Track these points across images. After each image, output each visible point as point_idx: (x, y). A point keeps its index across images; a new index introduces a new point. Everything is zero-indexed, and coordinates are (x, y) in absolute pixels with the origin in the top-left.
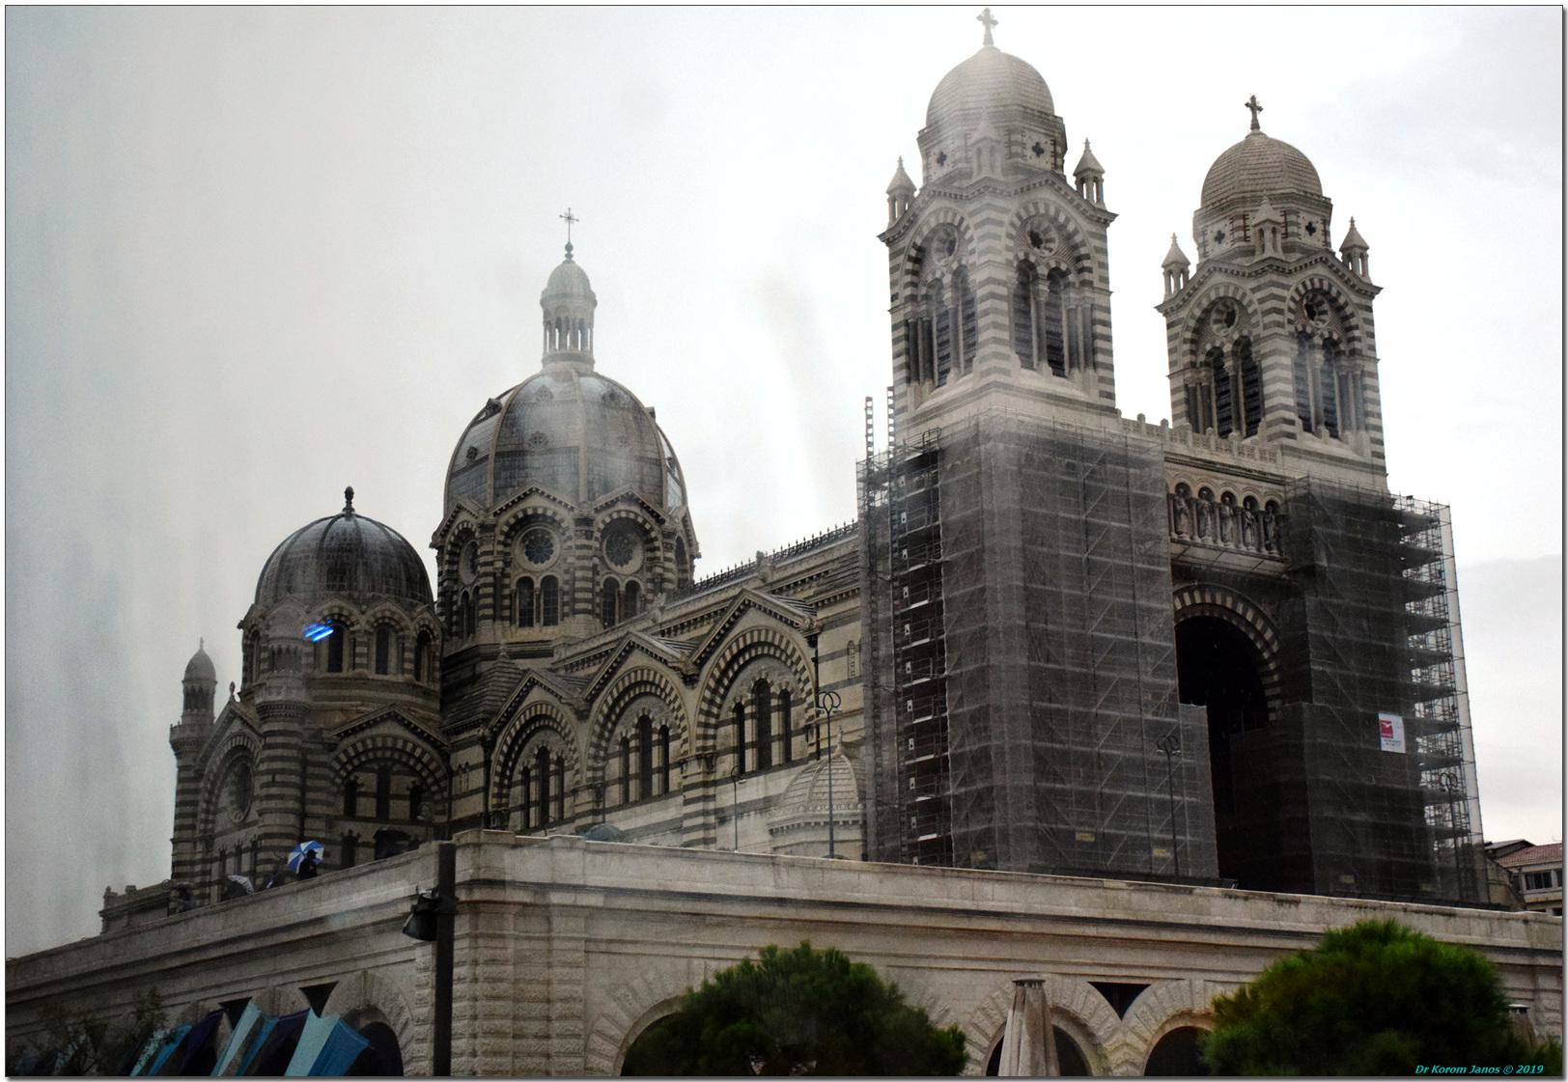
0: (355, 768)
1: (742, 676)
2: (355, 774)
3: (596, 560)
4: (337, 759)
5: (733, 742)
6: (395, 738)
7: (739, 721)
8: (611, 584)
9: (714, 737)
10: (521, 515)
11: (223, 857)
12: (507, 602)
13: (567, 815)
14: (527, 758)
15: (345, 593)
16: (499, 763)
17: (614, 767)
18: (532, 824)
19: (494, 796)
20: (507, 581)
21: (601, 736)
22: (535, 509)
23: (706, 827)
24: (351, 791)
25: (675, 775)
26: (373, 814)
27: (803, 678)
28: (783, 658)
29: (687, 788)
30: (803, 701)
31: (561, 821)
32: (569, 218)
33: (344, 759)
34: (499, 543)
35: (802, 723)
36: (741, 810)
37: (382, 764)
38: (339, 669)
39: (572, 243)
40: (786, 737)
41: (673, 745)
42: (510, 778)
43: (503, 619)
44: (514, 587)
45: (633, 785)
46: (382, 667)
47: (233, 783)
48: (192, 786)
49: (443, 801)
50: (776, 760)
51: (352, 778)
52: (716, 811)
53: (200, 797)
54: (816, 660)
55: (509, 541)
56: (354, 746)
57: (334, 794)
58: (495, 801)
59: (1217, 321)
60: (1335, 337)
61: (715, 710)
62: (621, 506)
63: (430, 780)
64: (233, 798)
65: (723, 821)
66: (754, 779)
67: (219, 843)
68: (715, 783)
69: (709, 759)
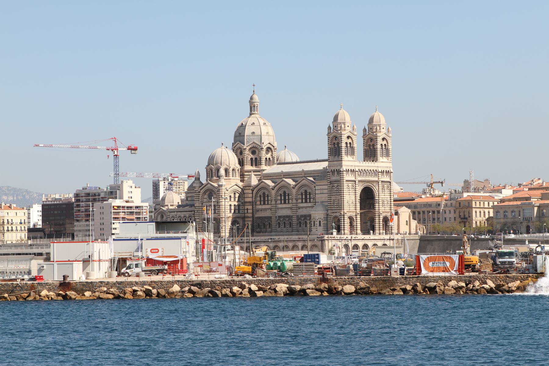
5: (301, 198)
7: (302, 195)
8: (266, 158)
17: (279, 198)
18: (262, 204)
23: (296, 209)
29: (292, 203)
31: (268, 204)
32: (254, 85)
36: (302, 207)
39: (255, 91)
40: (310, 198)
41: (290, 196)
44: (250, 159)
45: (283, 201)
48: (198, 194)
49: (243, 198)
52: (298, 207)
53: (200, 196)
62: (267, 145)
65: (299, 209)
68: (298, 203)
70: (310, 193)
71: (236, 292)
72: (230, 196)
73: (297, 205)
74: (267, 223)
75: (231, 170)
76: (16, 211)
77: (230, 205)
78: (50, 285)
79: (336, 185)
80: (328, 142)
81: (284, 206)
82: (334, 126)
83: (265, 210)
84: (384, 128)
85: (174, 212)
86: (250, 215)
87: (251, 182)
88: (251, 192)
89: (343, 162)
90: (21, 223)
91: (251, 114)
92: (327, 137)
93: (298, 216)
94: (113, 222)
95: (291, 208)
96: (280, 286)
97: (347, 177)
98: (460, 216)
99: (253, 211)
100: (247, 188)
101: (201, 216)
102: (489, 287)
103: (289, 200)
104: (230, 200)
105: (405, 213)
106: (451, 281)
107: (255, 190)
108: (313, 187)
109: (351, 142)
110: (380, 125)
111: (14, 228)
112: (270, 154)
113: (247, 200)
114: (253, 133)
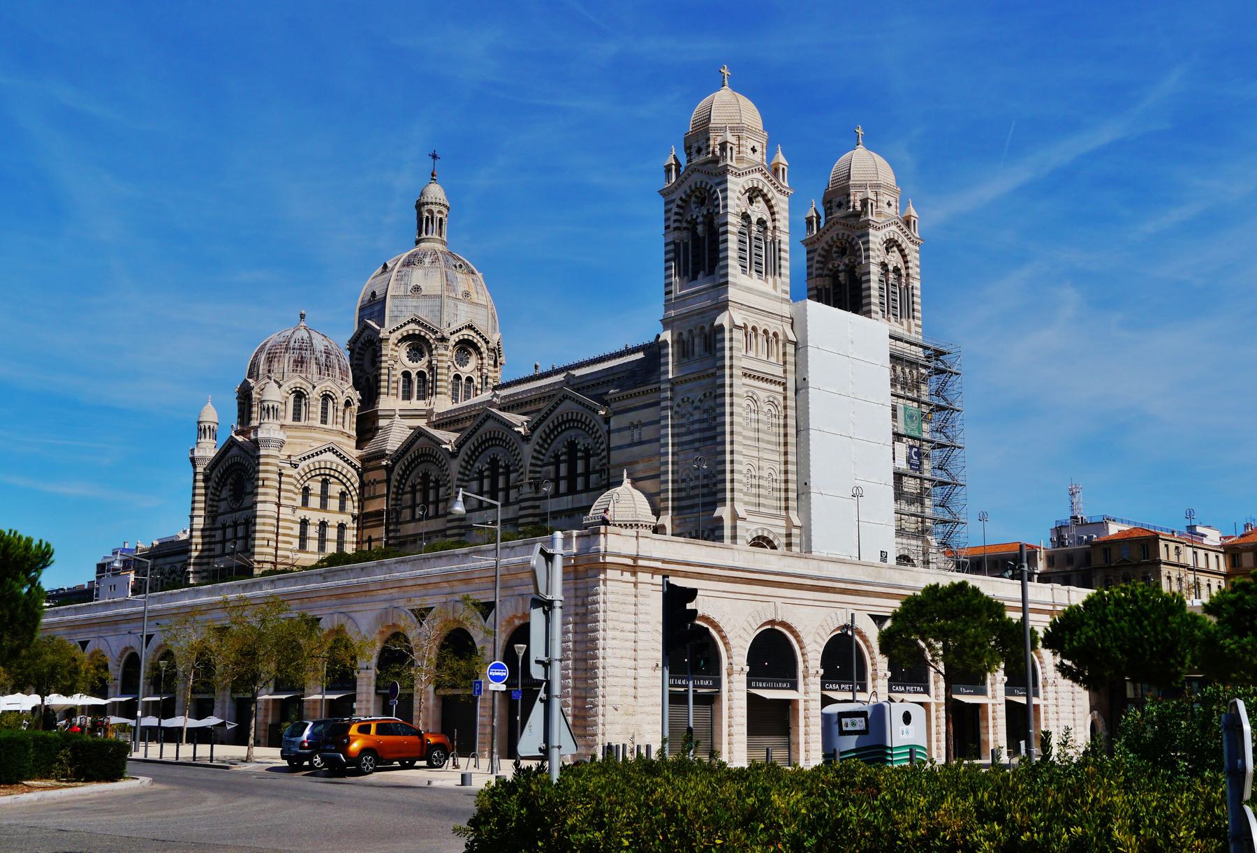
0: (308, 479)
1: (559, 439)
2: (308, 482)
3: (450, 363)
4: (299, 473)
5: (552, 476)
6: (332, 463)
8: (457, 377)
9: (540, 472)
10: (405, 334)
11: (224, 528)
12: (395, 385)
13: (441, 512)
14: (414, 478)
15: (303, 375)
16: (396, 480)
19: (393, 499)
20: (394, 372)
21: (465, 468)
22: (414, 330)
24: (306, 491)
25: (513, 494)
26: (318, 506)
27: (600, 441)
28: (587, 429)
30: (599, 454)
31: (437, 516)
32: (434, 157)
33: (303, 474)
34: (392, 350)
35: (598, 467)
37: (324, 477)
38: (299, 420)
39: (435, 173)
40: (587, 474)
42: (403, 489)
43: (393, 394)
46: (324, 421)
47: (231, 484)
50: (579, 487)
51: (306, 485)
53: (209, 491)
54: (609, 432)
55: (397, 349)
56: (308, 466)
57: (296, 494)
58: (393, 502)
59: (835, 252)
60: (899, 266)
61: (541, 457)
62: (465, 332)
63: (351, 488)
64: (232, 493)
66: (565, 498)
67: (220, 519)
69: (537, 486)
73: (538, 507)
75: (314, 395)
77: (304, 523)
80: (667, 220)
82: (694, 150)
84: (893, 203)
87: (385, 440)
88: (385, 478)
91: (418, 242)
92: (661, 201)
100: (373, 463)
101: (208, 564)
104: (305, 503)
107: (397, 468)
108: (602, 423)
110: (878, 186)
112: (473, 361)
114: (417, 289)
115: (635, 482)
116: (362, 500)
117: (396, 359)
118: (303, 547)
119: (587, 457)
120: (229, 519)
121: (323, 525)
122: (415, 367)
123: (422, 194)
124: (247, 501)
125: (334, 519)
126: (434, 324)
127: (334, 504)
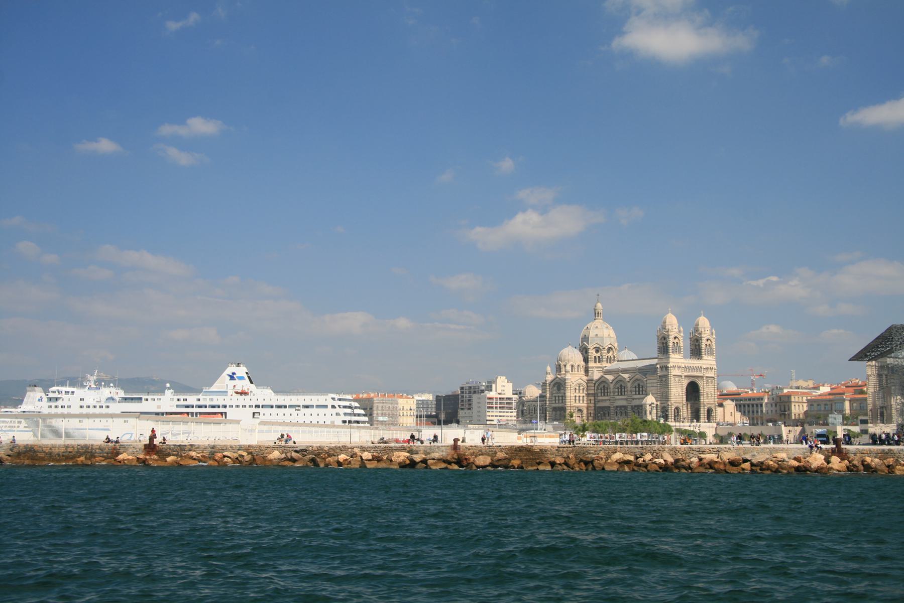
7: (636, 388)
8: (608, 357)
11: (555, 397)
17: (617, 390)
32: (598, 295)
36: (636, 399)
40: (642, 391)
46: (578, 372)
69: (631, 392)
70: (642, 386)
71: (341, 460)
72: (575, 388)
74: (606, 412)
76: (407, 400)
77: (575, 396)
78: (133, 448)
79: (664, 379)
81: (621, 397)
83: (605, 400)
85: (530, 401)
86: (592, 405)
89: (670, 359)
90: (411, 409)
91: (595, 319)
93: (632, 406)
94: (487, 410)
95: (626, 399)
96: (398, 455)
97: (674, 372)
98: (780, 409)
99: (595, 402)
100: (590, 382)
102: (664, 463)
103: (625, 392)
104: (575, 392)
105: (730, 405)
106: (616, 452)
107: (597, 384)
109: (678, 342)
111: (405, 414)
113: (591, 392)
114: (597, 335)
115: (652, 394)
116: (587, 390)
117: (592, 353)
118: (575, 402)
119: (642, 387)
120: (557, 395)
121: (579, 396)
122: (597, 355)
123: (595, 306)
124: (562, 391)
125: (581, 395)
126: (601, 345)
127: (581, 391)
